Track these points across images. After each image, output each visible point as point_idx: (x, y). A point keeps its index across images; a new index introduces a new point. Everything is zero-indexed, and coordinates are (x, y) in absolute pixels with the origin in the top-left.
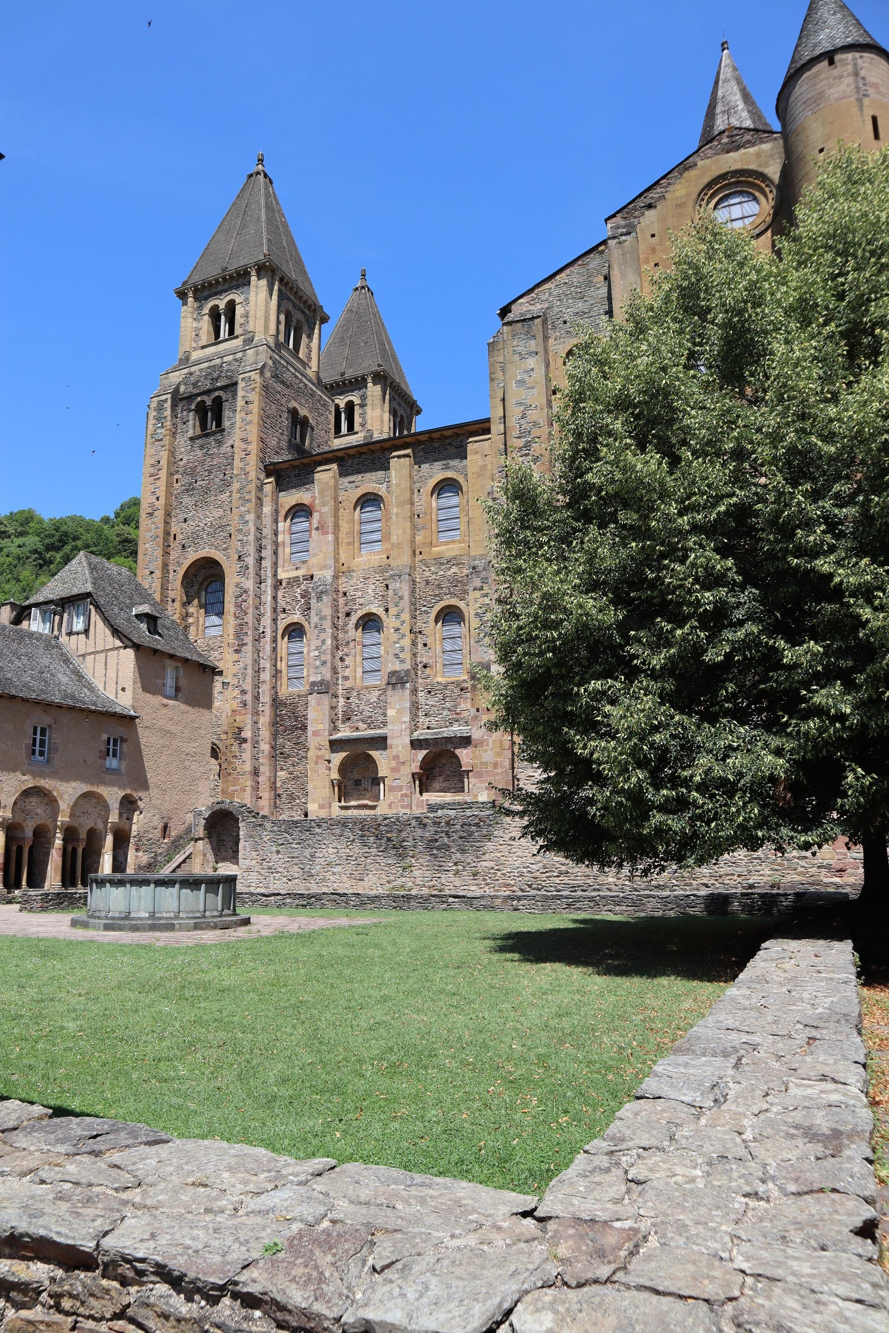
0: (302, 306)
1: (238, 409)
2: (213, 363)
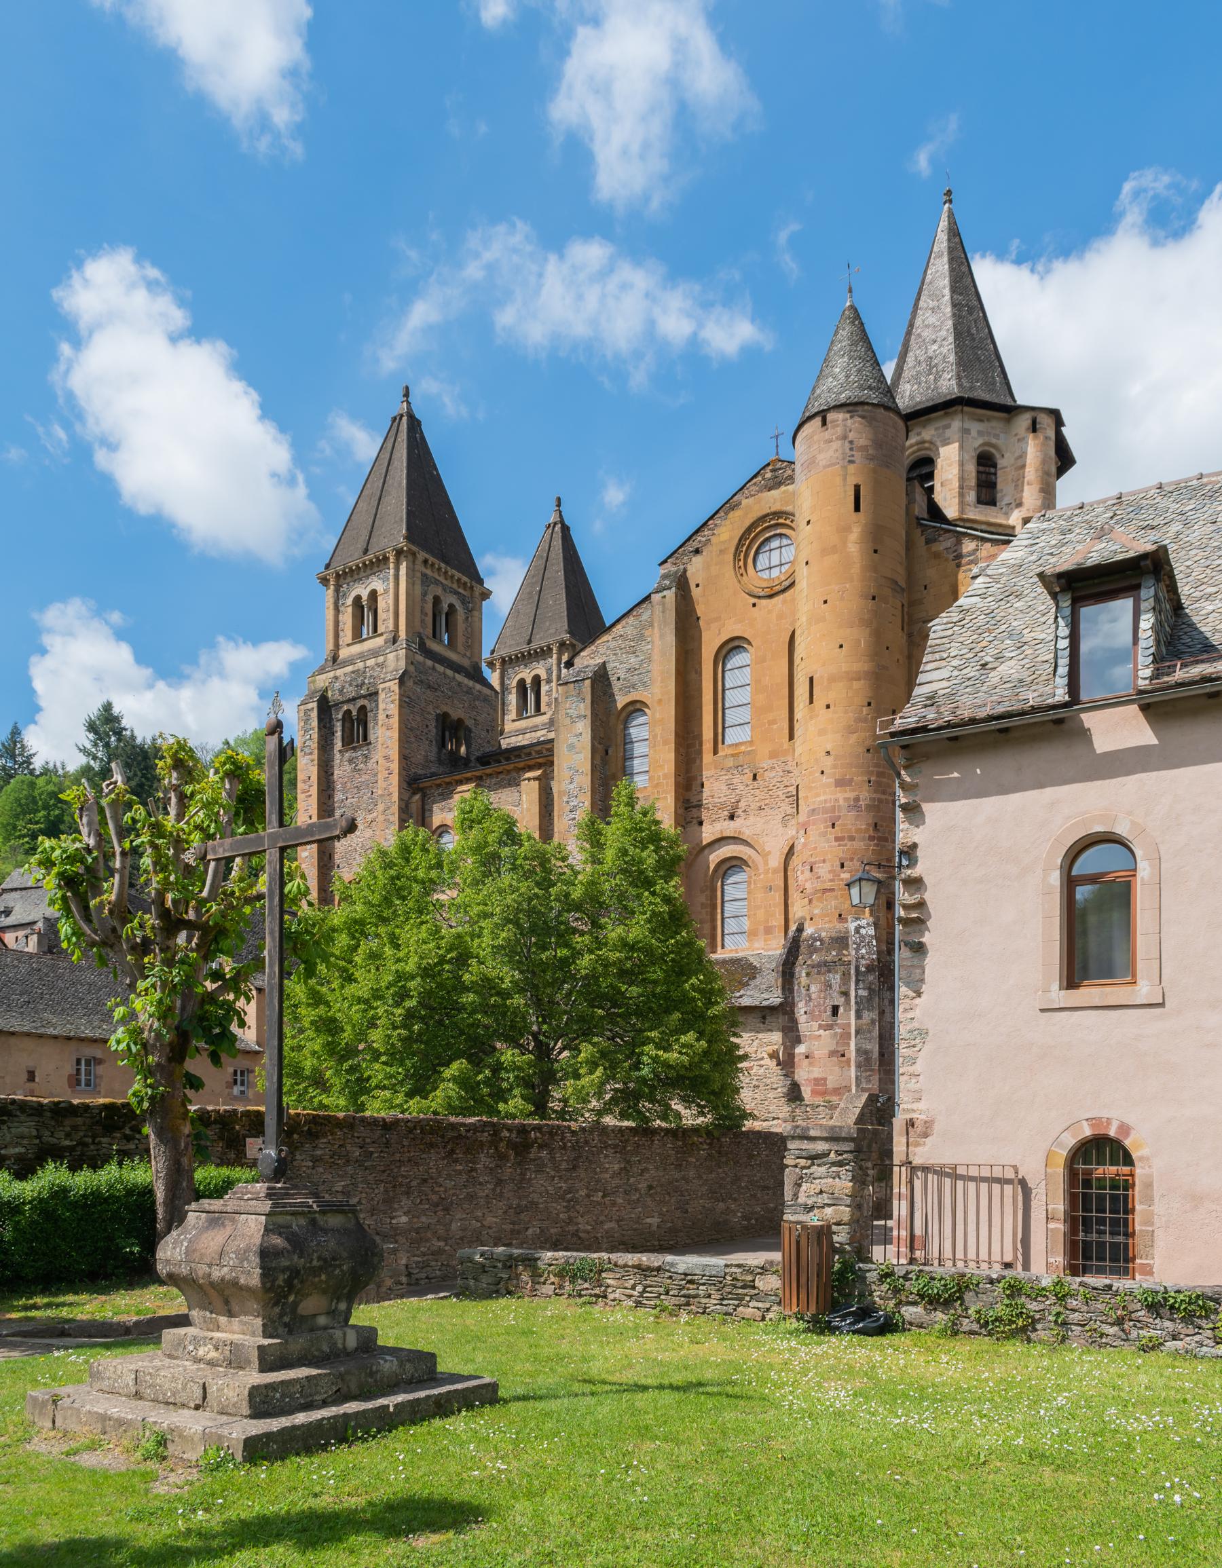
0: (455, 586)
1: (380, 723)
2: (356, 667)
